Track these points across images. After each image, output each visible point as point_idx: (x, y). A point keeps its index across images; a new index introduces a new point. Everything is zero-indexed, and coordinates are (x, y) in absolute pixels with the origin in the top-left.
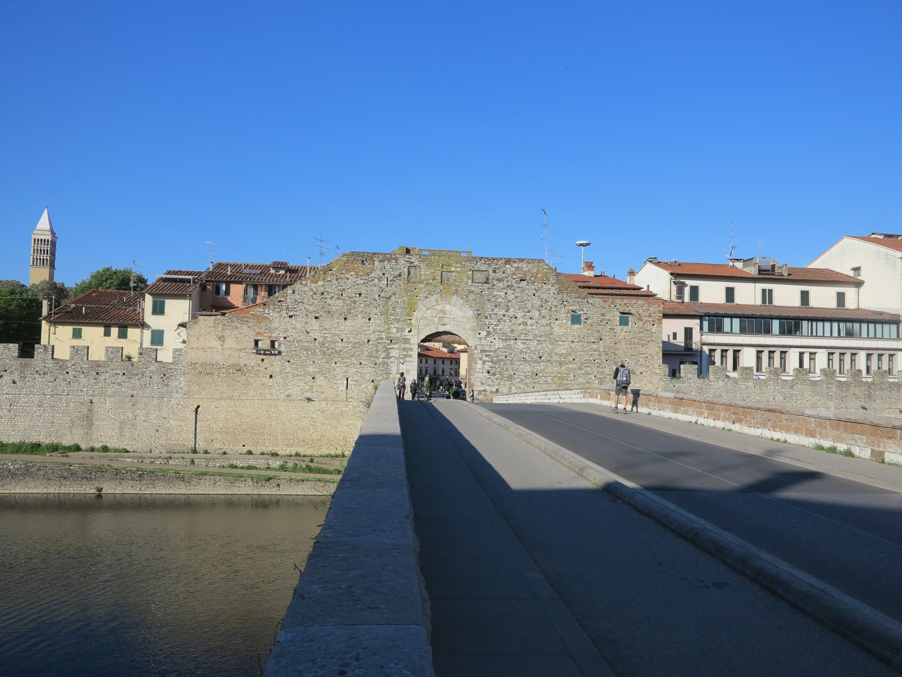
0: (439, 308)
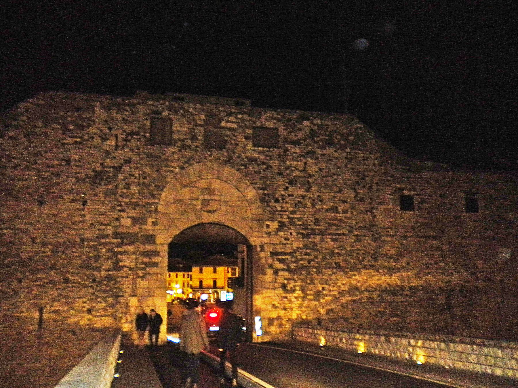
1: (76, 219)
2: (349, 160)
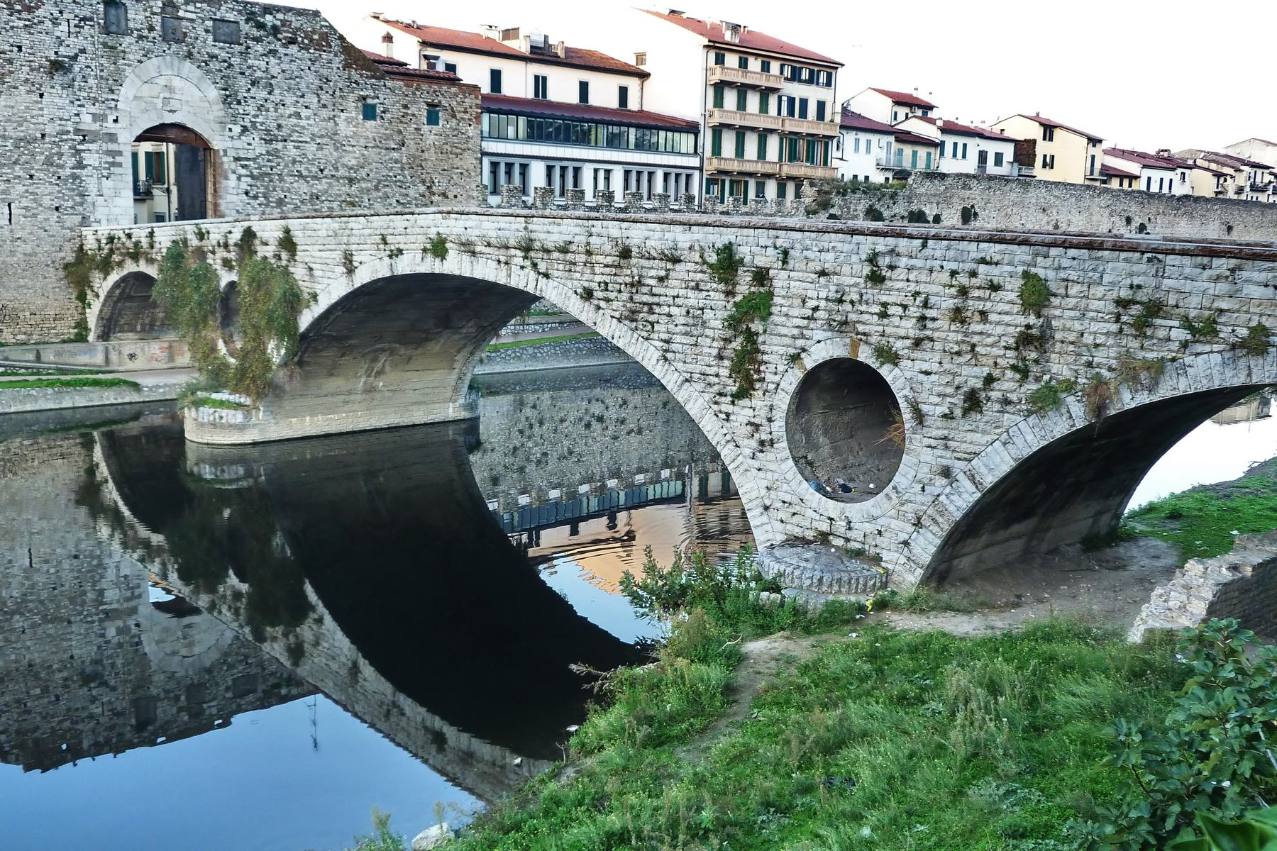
1: (35, 112)
2: (313, 62)
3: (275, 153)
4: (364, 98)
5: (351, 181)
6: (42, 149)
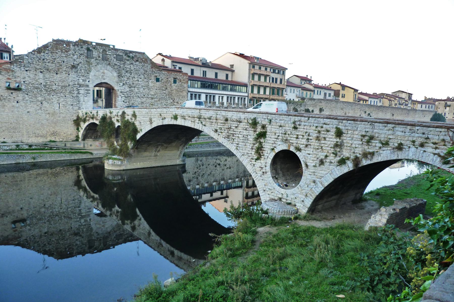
0: (102, 71)
3: (132, 91)
4: (156, 76)
5: (152, 98)
6: (69, 89)
